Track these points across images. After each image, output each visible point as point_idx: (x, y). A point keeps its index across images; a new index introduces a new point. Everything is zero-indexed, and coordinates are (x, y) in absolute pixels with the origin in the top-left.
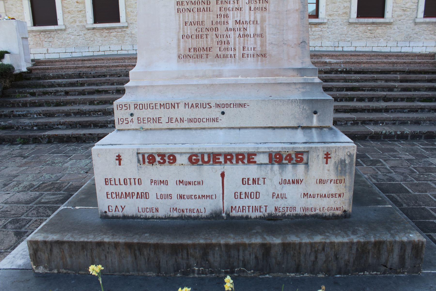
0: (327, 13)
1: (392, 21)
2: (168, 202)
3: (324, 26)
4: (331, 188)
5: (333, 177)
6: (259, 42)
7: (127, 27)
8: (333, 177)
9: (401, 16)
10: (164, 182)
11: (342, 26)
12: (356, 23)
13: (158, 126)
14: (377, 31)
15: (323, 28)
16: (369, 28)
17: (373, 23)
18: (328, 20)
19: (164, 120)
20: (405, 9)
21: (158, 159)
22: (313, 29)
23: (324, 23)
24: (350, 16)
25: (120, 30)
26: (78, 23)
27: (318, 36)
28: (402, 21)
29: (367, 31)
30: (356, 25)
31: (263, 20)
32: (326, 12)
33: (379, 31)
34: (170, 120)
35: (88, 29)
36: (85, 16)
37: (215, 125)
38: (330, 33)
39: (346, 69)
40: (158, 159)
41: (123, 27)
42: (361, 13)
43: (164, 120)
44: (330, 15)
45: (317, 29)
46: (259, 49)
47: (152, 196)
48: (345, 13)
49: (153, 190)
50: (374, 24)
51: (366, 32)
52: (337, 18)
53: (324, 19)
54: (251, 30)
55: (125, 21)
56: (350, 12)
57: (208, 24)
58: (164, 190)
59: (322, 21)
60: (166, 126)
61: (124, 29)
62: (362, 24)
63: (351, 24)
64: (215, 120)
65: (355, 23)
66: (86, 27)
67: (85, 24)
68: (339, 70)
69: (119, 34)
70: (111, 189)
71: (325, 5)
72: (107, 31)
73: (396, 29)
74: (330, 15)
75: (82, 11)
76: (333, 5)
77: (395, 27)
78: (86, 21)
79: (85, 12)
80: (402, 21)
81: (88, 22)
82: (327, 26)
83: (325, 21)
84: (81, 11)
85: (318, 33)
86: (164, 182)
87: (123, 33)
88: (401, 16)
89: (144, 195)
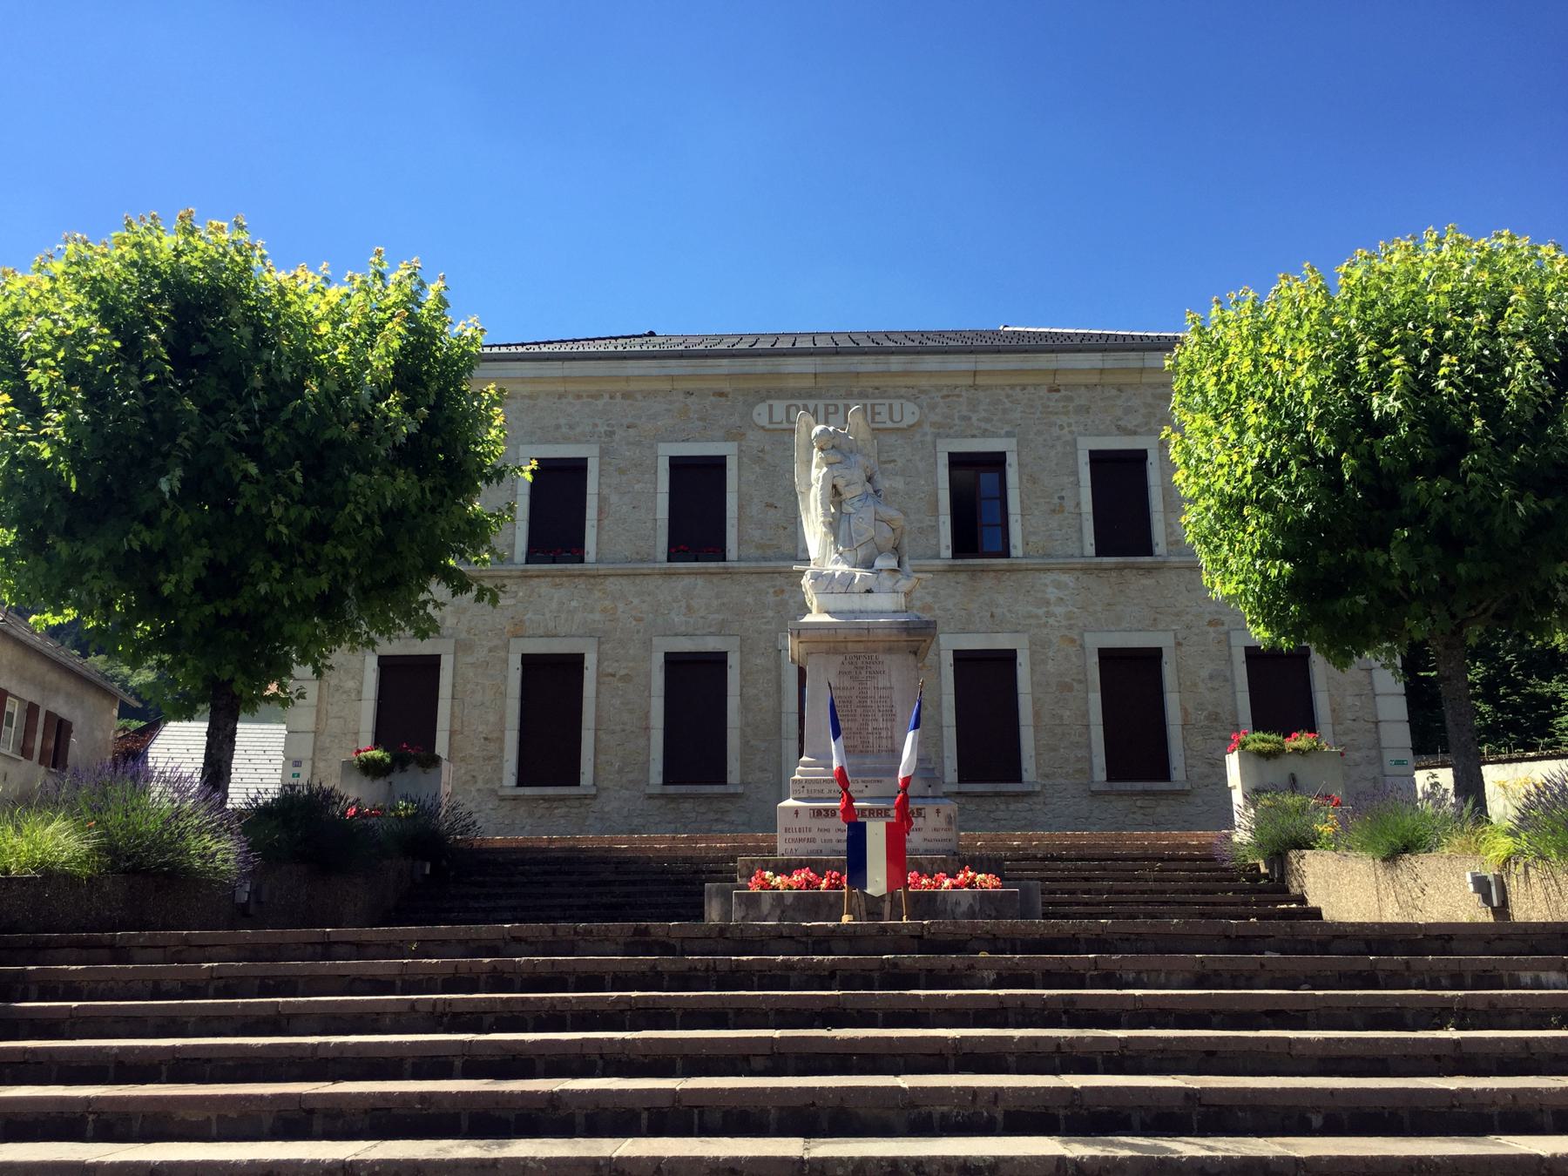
0: (1040, 771)
1: (1188, 787)
2: (829, 845)
3: (1035, 799)
4: (943, 835)
5: (944, 826)
6: (890, 742)
7: (595, 797)
8: (944, 826)
9: (1208, 776)
10: (828, 830)
11: (1078, 800)
12: (1106, 793)
13: (822, 795)
14: (1158, 809)
15: (1035, 803)
16: (1139, 803)
17: (1145, 793)
18: (1045, 785)
19: (826, 791)
20: (1212, 761)
21: (824, 813)
22: (1012, 807)
23: (1034, 792)
24: (1092, 777)
25: (577, 803)
26: (480, 785)
27: (1023, 822)
28: (1213, 787)
29: (1136, 809)
30: (1107, 798)
31: (892, 727)
32: (1037, 768)
33: (1163, 809)
34: (830, 791)
35: (503, 799)
36: (499, 769)
37: (862, 795)
38: (1050, 815)
39: (1052, 855)
40: (824, 813)
41: (585, 797)
42: (1114, 773)
43: (826, 791)
44: (1047, 776)
45: (1020, 805)
46: (889, 746)
47: (818, 841)
48: (1081, 771)
49: (819, 836)
50: (1148, 795)
51: (1134, 813)
52: (1063, 781)
53: (1033, 784)
54: (884, 734)
55: (591, 782)
56: (1091, 769)
57: (854, 730)
58: (828, 836)
59: (1030, 789)
60: (827, 795)
61: (587, 801)
62: (1120, 794)
63: (1095, 794)
64: (862, 791)
65: (1105, 791)
66: (500, 794)
67: (496, 786)
68: (1039, 856)
69: (573, 810)
70: (789, 836)
71: (1033, 753)
72: (546, 805)
73: (1201, 804)
74: (1047, 776)
75: (497, 758)
76: (1052, 754)
77: (1199, 801)
78: (501, 779)
79: (501, 761)
80: (1213, 787)
81: (505, 783)
82: (1041, 799)
83: (1038, 788)
84: (490, 759)
85: (1023, 814)
86: (828, 830)
87: (582, 810)
88: (1208, 776)
89: (813, 840)
